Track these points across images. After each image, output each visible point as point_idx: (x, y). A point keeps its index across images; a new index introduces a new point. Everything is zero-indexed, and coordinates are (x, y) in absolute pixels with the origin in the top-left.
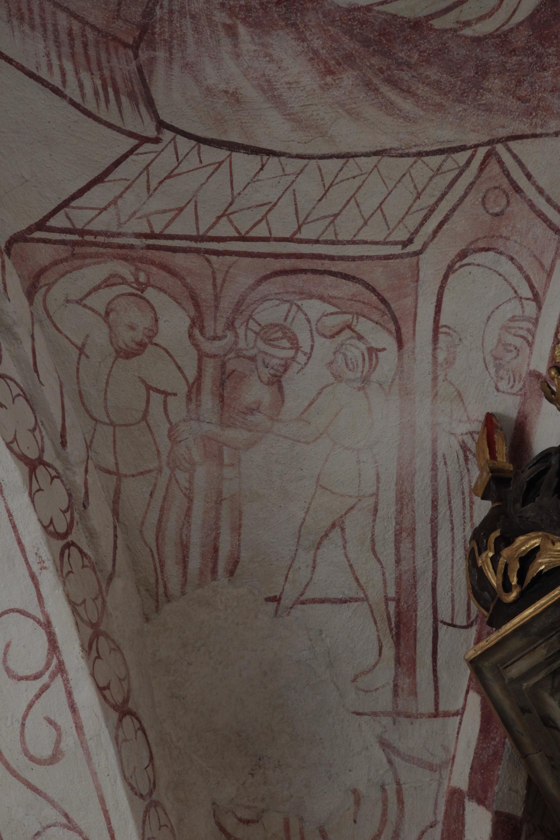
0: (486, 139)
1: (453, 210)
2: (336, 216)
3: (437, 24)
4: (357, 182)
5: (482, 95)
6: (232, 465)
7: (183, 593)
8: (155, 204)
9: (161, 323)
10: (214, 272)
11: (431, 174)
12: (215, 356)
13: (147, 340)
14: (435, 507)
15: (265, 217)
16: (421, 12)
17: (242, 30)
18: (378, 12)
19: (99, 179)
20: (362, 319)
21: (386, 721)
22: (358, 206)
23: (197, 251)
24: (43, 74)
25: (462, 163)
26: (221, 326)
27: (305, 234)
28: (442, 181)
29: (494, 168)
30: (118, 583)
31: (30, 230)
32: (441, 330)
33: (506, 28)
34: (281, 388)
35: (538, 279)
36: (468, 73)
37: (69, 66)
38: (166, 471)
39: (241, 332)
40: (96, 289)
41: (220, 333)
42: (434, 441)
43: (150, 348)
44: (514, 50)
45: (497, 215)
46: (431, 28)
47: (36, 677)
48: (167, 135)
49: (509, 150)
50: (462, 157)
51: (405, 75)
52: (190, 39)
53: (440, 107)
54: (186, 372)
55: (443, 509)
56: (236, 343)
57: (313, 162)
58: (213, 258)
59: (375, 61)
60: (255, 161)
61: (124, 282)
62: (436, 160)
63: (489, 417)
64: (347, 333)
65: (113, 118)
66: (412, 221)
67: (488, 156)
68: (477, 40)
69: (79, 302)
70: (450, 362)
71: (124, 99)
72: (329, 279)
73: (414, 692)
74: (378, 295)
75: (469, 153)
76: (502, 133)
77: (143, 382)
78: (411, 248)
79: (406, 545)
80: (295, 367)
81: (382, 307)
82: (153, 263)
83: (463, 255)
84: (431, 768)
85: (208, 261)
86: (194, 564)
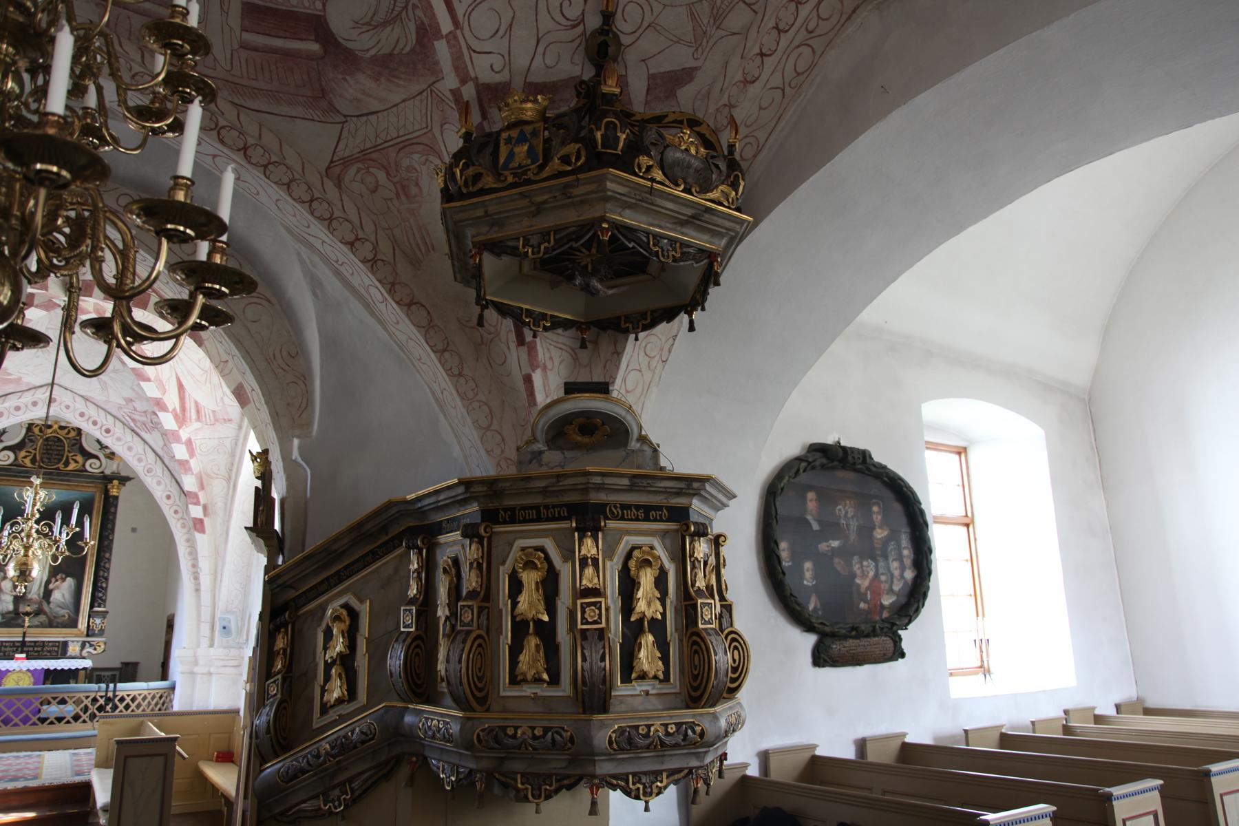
3: (396, 52)
15: (388, 133)
17: (347, 78)
19: (339, 140)
24: (306, 117)
37: (311, 111)
40: (355, 175)
45: (442, 111)
48: (348, 118)
50: (425, 94)
57: (390, 111)
61: (362, 169)
62: (419, 97)
65: (331, 120)
66: (424, 119)
68: (408, 54)
72: (415, 146)
76: (430, 82)
83: (442, 127)
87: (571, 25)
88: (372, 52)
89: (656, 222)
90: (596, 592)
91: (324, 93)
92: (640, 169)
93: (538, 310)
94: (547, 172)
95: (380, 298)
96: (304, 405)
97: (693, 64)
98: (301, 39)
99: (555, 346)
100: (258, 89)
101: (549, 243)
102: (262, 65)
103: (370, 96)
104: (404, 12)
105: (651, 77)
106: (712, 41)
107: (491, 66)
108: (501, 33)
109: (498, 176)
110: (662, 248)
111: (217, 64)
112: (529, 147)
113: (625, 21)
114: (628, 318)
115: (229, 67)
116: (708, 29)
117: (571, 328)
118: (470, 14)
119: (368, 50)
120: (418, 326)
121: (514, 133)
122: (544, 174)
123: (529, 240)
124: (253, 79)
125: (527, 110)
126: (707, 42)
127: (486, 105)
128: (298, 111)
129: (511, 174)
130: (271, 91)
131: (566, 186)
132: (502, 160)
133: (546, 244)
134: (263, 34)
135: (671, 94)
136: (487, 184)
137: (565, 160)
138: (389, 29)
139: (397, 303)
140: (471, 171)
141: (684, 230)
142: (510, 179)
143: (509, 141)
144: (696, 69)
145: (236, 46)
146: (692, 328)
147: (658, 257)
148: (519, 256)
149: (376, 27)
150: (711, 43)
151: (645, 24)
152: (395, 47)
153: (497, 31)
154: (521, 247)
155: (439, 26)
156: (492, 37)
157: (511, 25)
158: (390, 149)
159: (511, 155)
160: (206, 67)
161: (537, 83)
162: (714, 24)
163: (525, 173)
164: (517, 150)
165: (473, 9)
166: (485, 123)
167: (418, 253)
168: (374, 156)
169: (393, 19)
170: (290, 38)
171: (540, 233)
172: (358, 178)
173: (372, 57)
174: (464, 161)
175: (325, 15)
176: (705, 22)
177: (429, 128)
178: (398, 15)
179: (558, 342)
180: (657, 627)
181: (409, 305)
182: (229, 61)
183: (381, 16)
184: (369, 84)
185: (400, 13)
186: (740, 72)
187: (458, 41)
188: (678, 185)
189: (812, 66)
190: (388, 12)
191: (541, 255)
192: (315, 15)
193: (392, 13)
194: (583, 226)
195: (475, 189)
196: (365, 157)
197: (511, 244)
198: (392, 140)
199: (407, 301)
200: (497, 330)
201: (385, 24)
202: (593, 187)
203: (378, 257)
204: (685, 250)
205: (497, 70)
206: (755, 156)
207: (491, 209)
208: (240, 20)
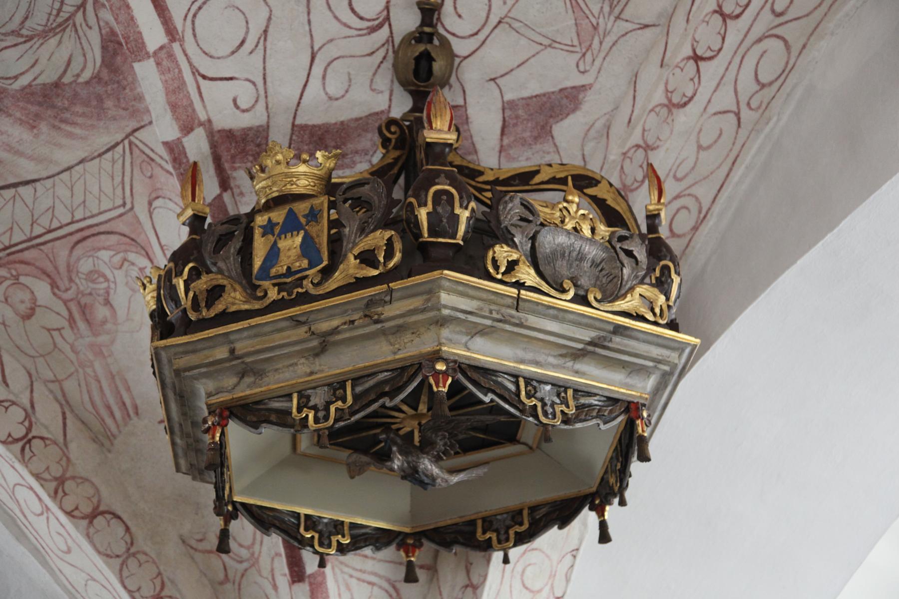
0: (124, 135)
1: (132, 180)
2: (84, 202)
4: (82, 181)
5: (107, 113)
6: (110, 356)
7: (120, 432)
9: (36, 293)
10: (47, 255)
11: (111, 164)
12: (72, 300)
13: (33, 306)
15: (53, 215)
18: (36, 85)
20: (129, 253)
22: (90, 193)
23: (33, 247)
25: (121, 152)
26: (67, 282)
29: (136, 152)
30: (73, 446)
32: (165, 248)
33: (96, 71)
34: (111, 305)
36: (94, 103)
38: (81, 370)
39: (77, 281)
41: (68, 286)
43: (37, 309)
44: (106, 83)
45: (151, 177)
46: (64, 85)
49: (137, 138)
50: (119, 149)
51: (67, 115)
54: (62, 314)
56: (78, 288)
57: (56, 178)
58: (42, 247)
59: (49, 112)
61: (6, 279)
62: (109, 154)
64: (126, 264)
66: (119, 191)
67: (131, 143)
68: (87, 83)
72: (102, 237)
74: (129, 237)
75: (121, 146)
76: (129, 130)
77: (44, 328)
80: (112, 292)
81: (133, 243)
82: (15, 262)
85: (41, 250)
86: (118, 414)
87: (368, 28)
88: (24, 81)
89: (529, 356)
92: (497, 268)
93: (328, 515)
94: (337, 279)
97: (577, 80)
99: (359, 579)
101: (344, 400)
105: (508, 106)
107: (235, 101)
108: (249, 46)
109: (251, 288)
110: (542, 400)
112: (304, 239)
113: (460, 16)
114: (488, 523)
116: (601, 20)
117: (388, 544)
118: (195, 16)
119: (16, 78)
120: (107, 556)
121: (278, 216)
122: (332, 284)
123: (308, 398)
125: (298, 176)
126: (601, 43)
127: (227, 166)
129: (274, 285)
131: (371, 302)
132: (257, 263)
133: (339, 404)
135: (543, 132)
136: (233, 304)
137: (367, 258)
138: (53, 41)
139: (69, 514)
140: (203, 283)
141: (578, 366)
142: (273, 294)
143: (269, 228)
144: (583, 88)
146: (604, 537)
147: (536, 417)
148: (292, 426)
149: (30, 39)
151: (493, 20)
152: (65, 71)
153: (243, 42)
154: (294, 410)
155: (142, 38)
156: (233, 53)
157: (265, 32)
158: (58, 243)
159: (273, 254)
161: (314, 126)
162: (610, 14)
163: (299, 282)
164: (283, 244)
165: (200, 8)
166: (227, 197)
167: (109, 421)
168: (27, 255)
169: (60, 25)
171: (328, 385)
173: (23, 89)
174: (191, 265)
176: (596, 10)
177: (128, 206)
178: (67, 20)
179: (363, 572)
181: (92, 517)
183: (38, 20)
184: (17, 133)
185: (72, 15)
186: (661, 88)
187: (175, 61)
188: (564, 291)
189: (786, 72)
190: (50, 14)
191: (331, 421)
193: (58, 15)
194: (403, 369)
195: (212, 313)
197: (276, 405)
198: (60, 227)
199: (87, 509)
200: (253, 554)
201: (46, 33)
202: (416, 303)
203: (34, 433)
204: (583, 401)
205: (243, 106)
206: (695, 228)
207: (242, 347)
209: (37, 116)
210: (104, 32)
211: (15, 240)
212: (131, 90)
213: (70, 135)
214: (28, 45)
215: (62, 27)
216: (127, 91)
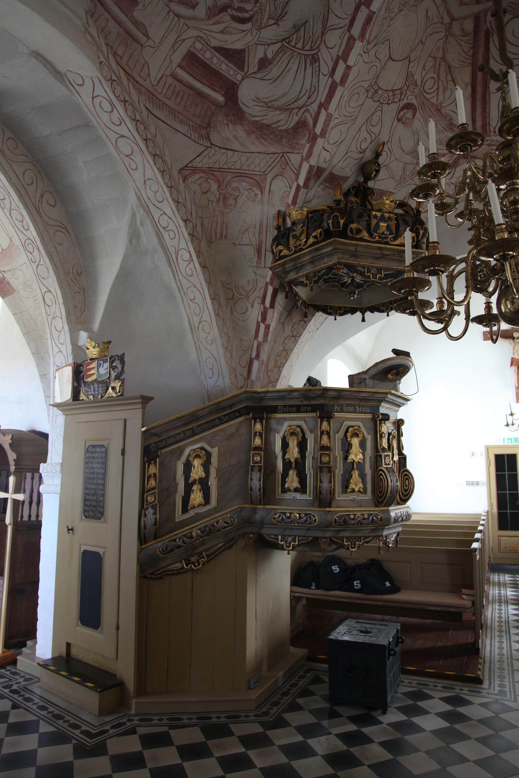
1: (274, 166)
3: (273, 126)
8: (210, 161)
14: (267, 228)
16: (269, 123)
17: (230, 124)
19: (198, 156)
21: (255, 268)
24: (187, 134)
26: (224, 186)
27: (243, 168)
28: (272, 160)
29: (283, 159)
30: (203, 242)
31: (184, 167)
34: (236, 201)
35: (291, 184)
36: (279, 137)
37: (192, 133)
39: (228, 189)
40: (198, 179)
42: (268, 214)
45: (283, 169)
47: (188, 261)
48: (213, 146)
50: (277, 155)
51: (266, 137)
52: (219, 126)
53: (273, 144)
55: (268, 229)
59: (259, 133)
60: (232, 153)
61: (204, 178)
62: (271, 155)
63: (279, 211)
64: (251, 190)
65: (201, 143)
66: (266, 168)
67: (282, 156)
68: (281, 131)
69: (194, 182)
70: (272, 198)
71: (204, 139)
72: (247, 178)
73: (261, 263)
76: (285, 151)
78: (265, 173)
79: (261, 235)
80: (239, 197)
83: (276, 176)
84: (263, 277)
86: (218, 236)
88: (257, 119)
90: (328, 448)
91: (209, 125)
95: (187, 257)
96: (83, 309)
97: (392, 190)
98: (214, 90)
100: (167, 105)
102: (179, 92)
103: (237, 140)
104: (297, 110)
106: (406, 184)
108: (337, 144)
111: (148, 78)
114: (331, 308)
115: (155, 83)
119: (254, 116)
124: (167, 98)
128: (184, 129)
130: (175, 110)
134: (190, 75)
138: (278, 112)
145: (168, 73)
146: (363, 320)
149: (270, 107)
150: (404, 185)
158: (230, 174)
160: (139, 76)
167: (214, 237)
169: (286, 109)
170: (207, 85)
172: (198, 182)
175: (239, 85)
176: (408, 173)
177: (266, 173)
178: (290, 109)
180: (361, 466)
182: (157, 80)
185: (294, 109)
190: (284, 104)
192: (233, 81)
196: (210, 172)
200: (248, 294)
208: (181, 59)
209: (253, 132)
210: (301, 119)
211: (215, 166)
212: (297, 140)
213: (262, 143)
214: (267, 109)
215: (286, 110)
216: (296, 140)
